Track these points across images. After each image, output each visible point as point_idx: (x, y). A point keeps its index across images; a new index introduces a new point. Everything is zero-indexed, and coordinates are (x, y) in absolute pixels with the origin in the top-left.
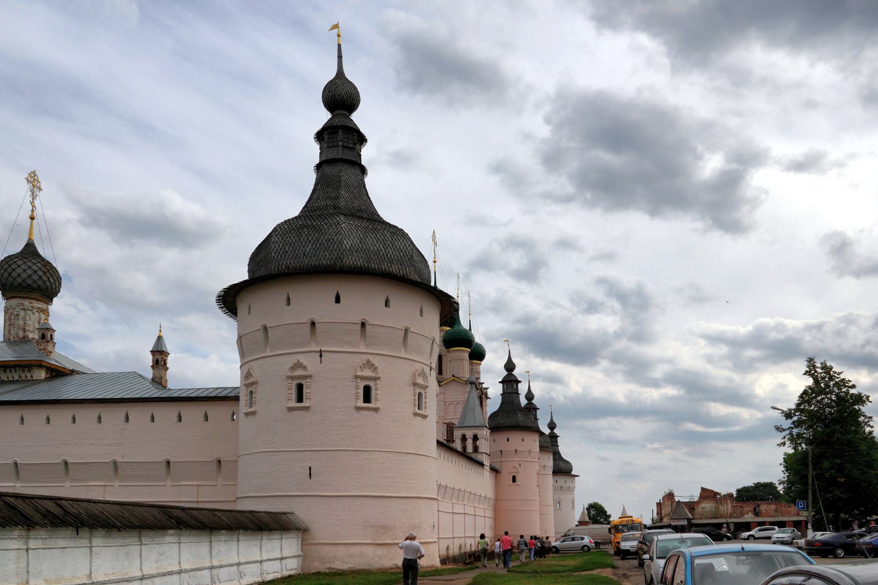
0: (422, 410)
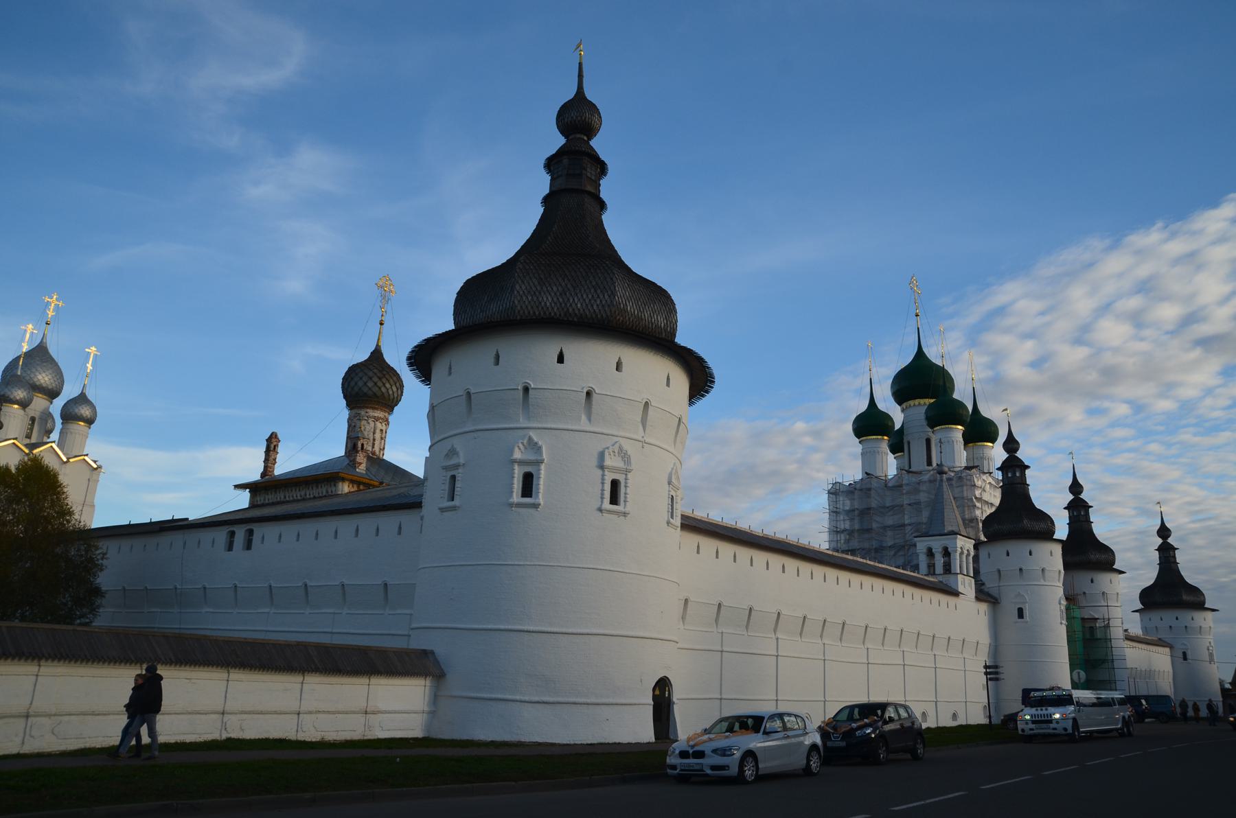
0: (619, 505)
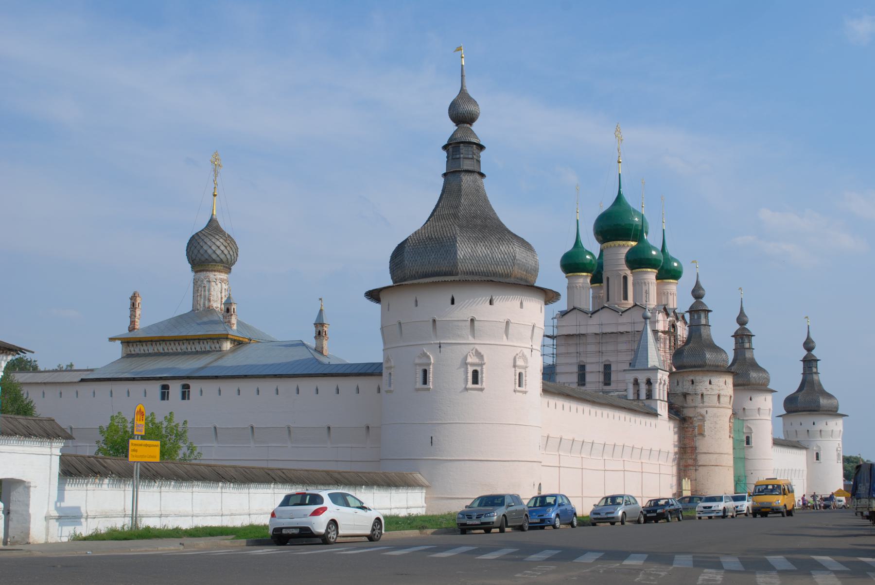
0: (522, 387)
